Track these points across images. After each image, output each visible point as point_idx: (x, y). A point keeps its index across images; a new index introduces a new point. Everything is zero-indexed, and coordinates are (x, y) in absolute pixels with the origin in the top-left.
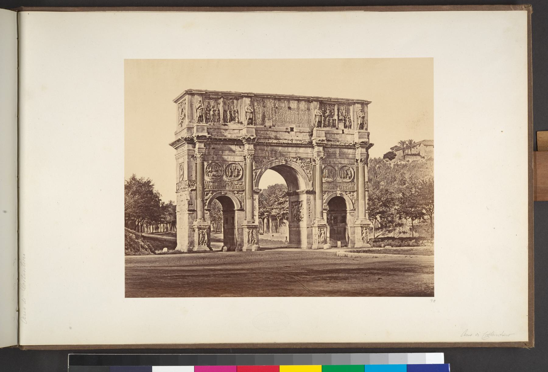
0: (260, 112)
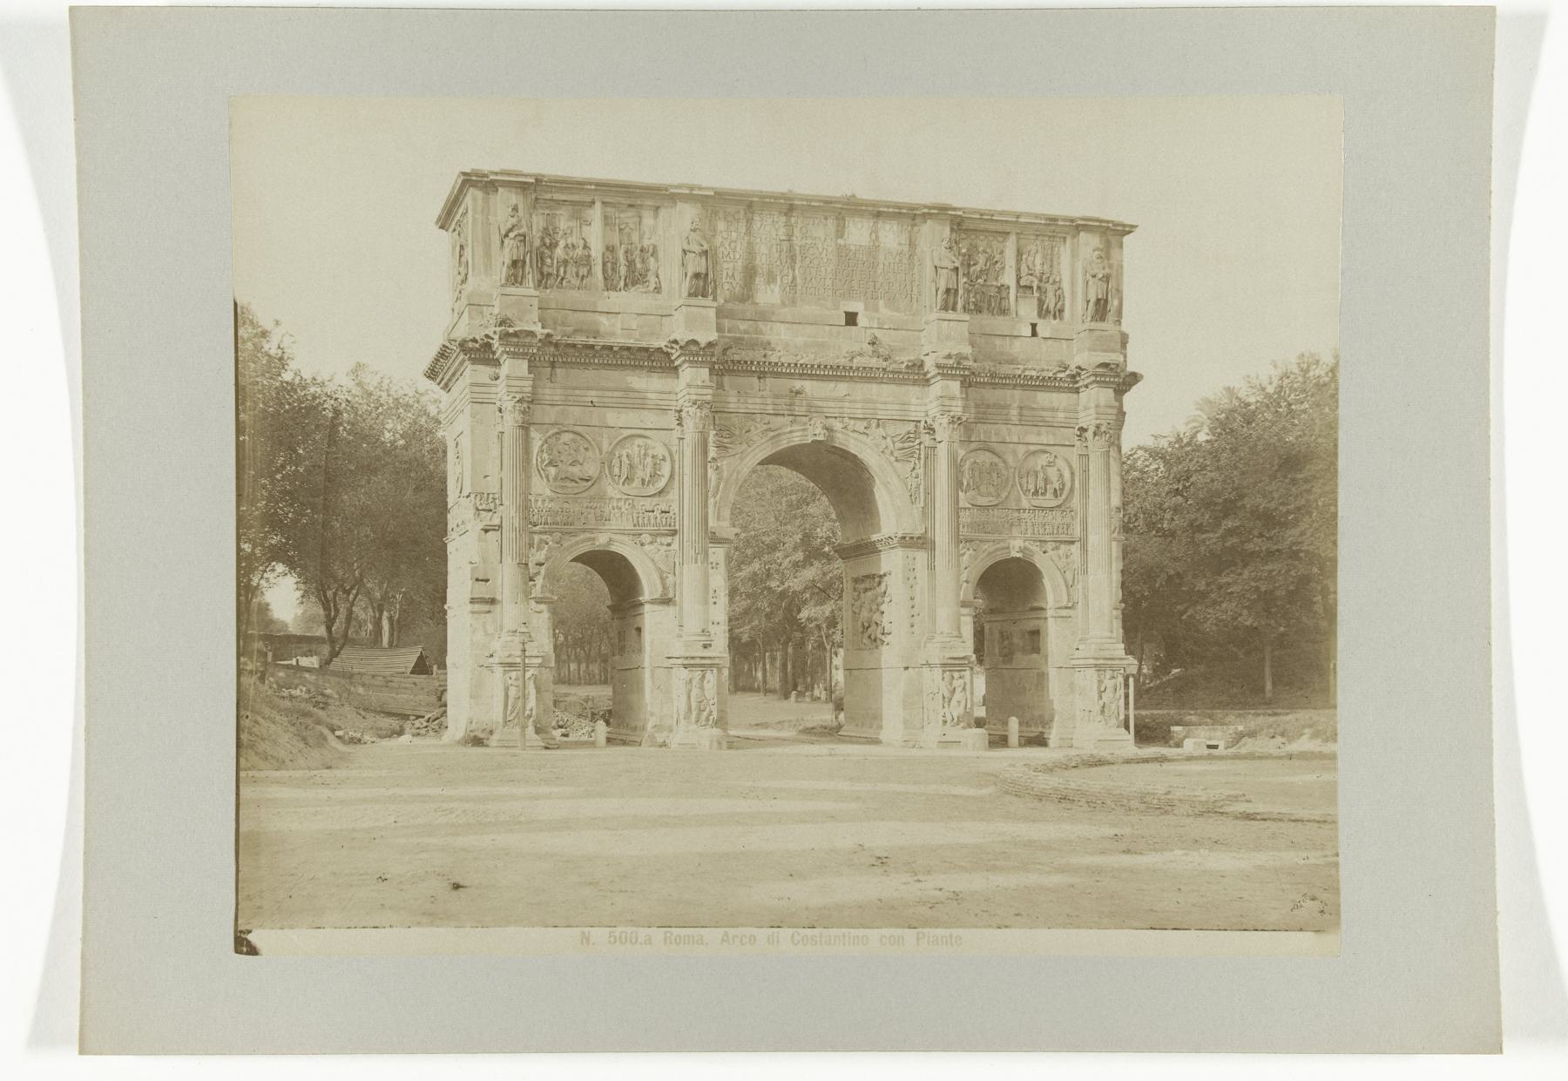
0: (738, 256)
